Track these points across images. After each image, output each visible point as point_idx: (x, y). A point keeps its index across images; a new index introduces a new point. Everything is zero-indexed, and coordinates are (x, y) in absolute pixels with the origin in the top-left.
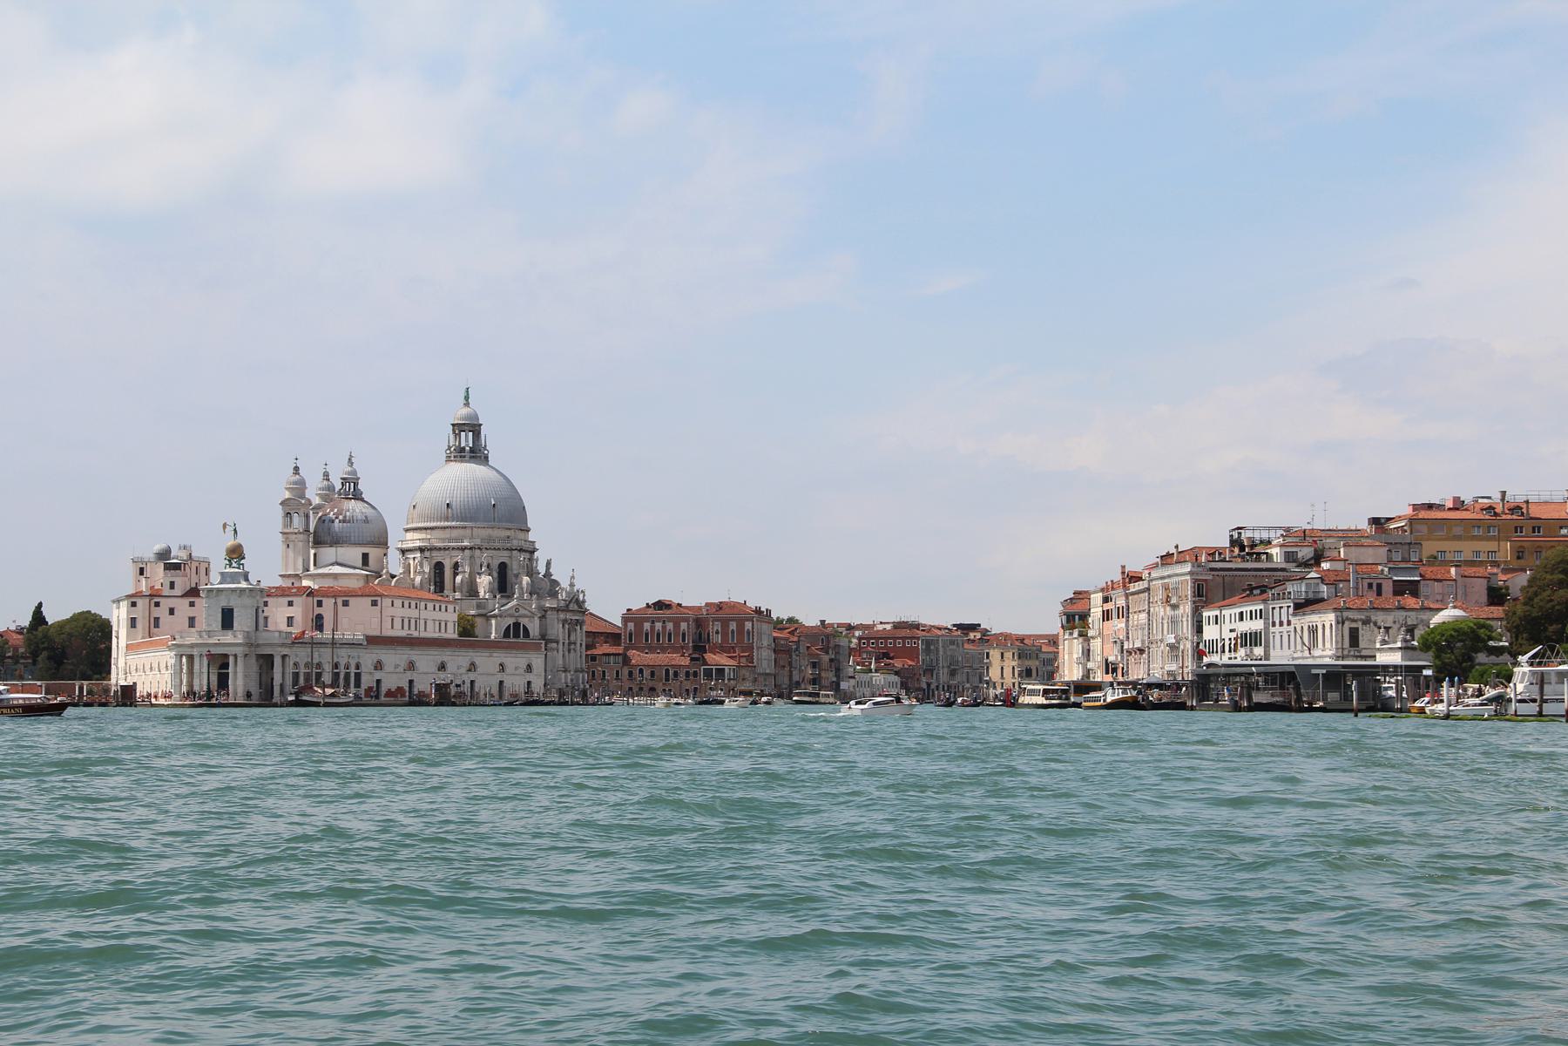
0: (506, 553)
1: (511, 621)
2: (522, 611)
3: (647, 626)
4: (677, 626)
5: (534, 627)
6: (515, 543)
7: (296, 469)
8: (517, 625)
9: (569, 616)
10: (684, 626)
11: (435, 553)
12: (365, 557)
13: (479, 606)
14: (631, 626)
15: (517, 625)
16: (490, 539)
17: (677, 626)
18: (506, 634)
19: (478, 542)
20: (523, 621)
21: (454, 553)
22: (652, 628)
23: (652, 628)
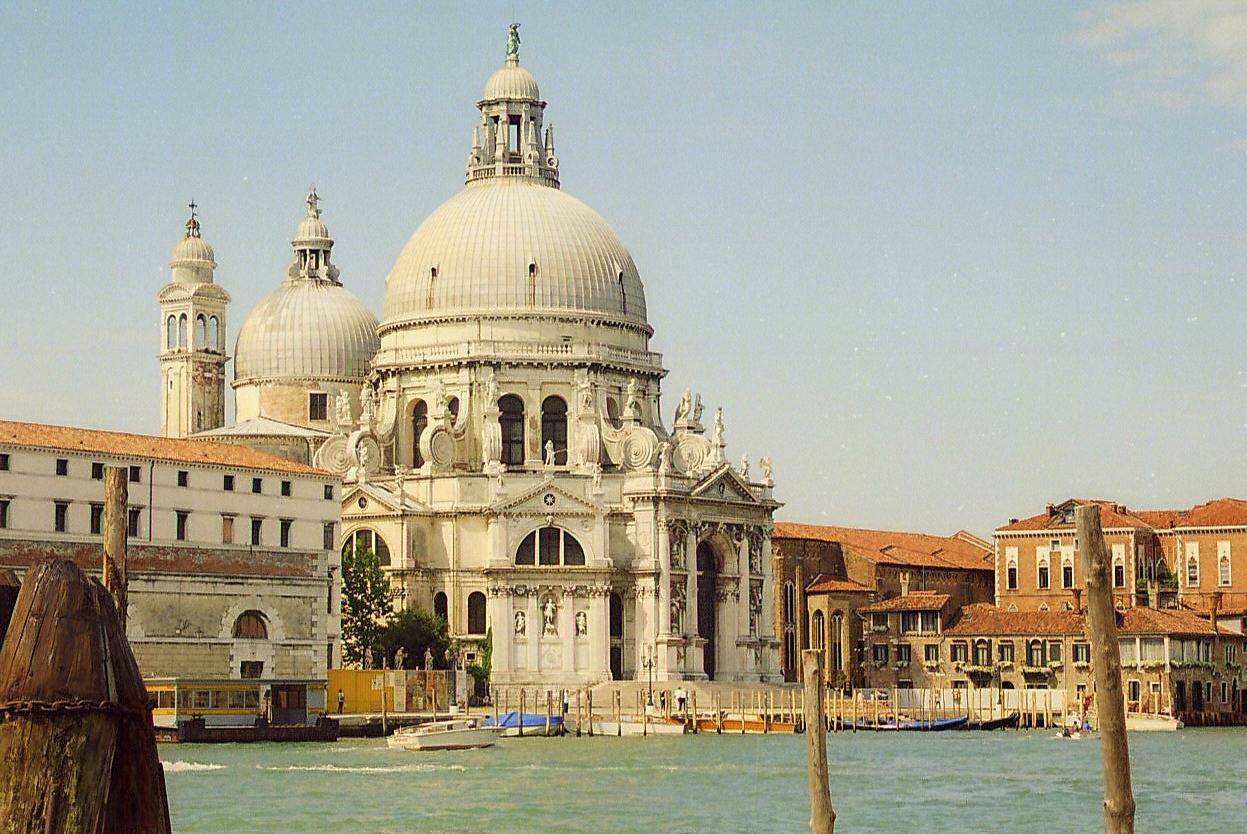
0: (560, 375)
1: (535, 525)
3: (1043, 553)
6: (579, 353)
7: (196, 225)
8: (550, 535)
9: (694, 515)
14: (1012, 554)
15: (550, 535)
18: (524, 552)
21: (449, 377)
22: (1055, 557)
23: (1055, 557)
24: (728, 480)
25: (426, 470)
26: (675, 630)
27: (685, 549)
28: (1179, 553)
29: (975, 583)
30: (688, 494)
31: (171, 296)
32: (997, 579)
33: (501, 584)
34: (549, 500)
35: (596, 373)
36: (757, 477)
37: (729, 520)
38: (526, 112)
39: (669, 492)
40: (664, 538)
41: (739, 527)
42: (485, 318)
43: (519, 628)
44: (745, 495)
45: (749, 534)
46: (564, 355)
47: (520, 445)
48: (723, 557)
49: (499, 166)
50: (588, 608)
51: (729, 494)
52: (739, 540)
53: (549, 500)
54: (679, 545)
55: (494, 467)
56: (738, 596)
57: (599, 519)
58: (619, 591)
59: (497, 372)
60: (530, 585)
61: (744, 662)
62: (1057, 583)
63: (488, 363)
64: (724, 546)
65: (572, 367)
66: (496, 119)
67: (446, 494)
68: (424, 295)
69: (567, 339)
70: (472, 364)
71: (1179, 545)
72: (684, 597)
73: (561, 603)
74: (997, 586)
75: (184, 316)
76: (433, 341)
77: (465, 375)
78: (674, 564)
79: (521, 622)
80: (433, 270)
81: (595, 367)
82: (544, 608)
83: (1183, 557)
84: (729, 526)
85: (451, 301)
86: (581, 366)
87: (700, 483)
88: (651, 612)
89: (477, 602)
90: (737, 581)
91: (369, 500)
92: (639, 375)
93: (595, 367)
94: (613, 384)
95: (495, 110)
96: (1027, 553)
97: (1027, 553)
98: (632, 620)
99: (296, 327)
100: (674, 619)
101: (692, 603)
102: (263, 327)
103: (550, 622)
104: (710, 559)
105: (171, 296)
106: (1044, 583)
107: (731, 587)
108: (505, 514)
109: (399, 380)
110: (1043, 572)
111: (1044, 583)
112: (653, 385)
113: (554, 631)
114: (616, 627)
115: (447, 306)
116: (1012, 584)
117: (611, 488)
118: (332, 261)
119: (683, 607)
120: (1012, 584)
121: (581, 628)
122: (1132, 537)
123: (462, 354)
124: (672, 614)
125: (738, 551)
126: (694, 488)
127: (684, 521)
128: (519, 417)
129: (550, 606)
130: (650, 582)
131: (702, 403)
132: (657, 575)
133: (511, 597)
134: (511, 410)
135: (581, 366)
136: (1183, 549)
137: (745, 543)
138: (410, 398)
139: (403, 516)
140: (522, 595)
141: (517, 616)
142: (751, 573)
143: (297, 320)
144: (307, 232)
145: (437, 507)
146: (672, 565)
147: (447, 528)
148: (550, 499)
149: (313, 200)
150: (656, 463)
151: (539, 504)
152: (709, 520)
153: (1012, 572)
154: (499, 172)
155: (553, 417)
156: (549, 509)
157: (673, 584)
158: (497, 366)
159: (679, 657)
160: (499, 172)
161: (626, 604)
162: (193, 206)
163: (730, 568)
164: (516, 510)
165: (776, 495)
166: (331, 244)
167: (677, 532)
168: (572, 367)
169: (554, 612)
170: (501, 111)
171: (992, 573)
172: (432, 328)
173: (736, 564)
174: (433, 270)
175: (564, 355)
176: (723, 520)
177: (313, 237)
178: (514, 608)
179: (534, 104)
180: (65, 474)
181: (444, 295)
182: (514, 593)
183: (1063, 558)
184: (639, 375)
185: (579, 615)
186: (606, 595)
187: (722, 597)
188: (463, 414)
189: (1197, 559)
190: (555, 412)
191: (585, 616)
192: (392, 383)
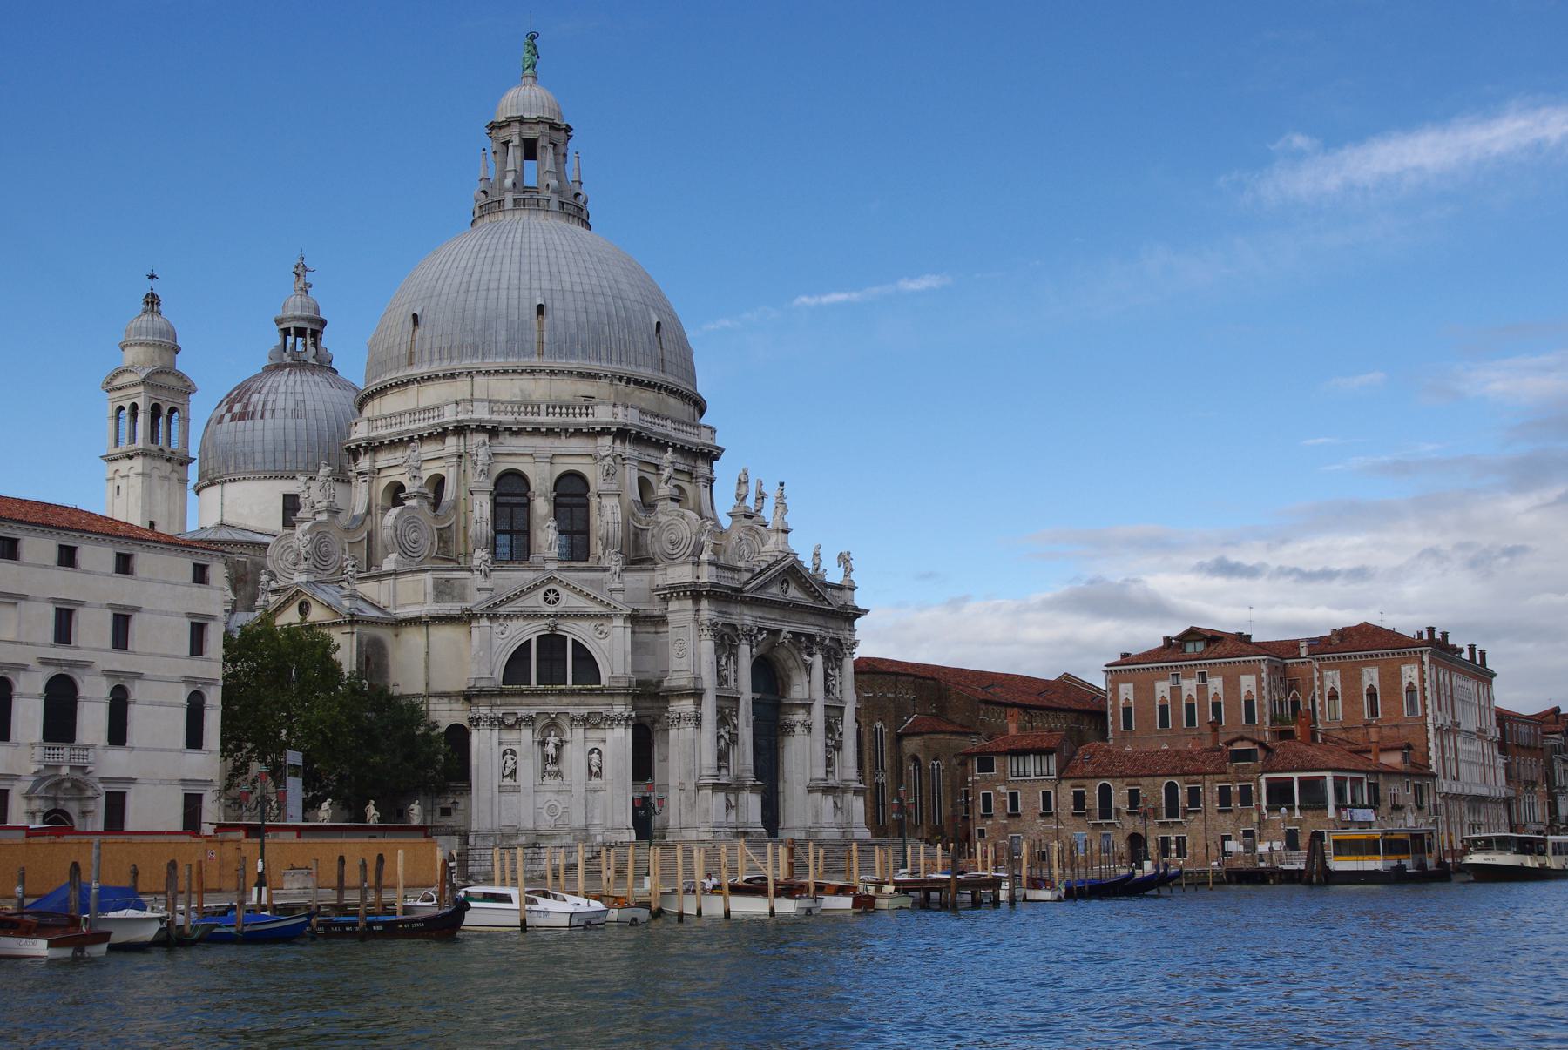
1: (530, 631)
2: (569, 601)
3: (1163, 688)
4: (1232, 684)
5: (613, 650)
6: (603, 415)
8: (552, 644)
9: (746, 618)
10: (1248, 683)
11: (384, 459)
12: (291, 504)
13: (442, 591)
14: (1126, 691)
15: (552, 644)
16: (530, 406)
17: (1232, 684)
19: (482, 413)
20: (576, 631)
21: (429, 450)
22: (1176, 691)
23: (1176, 691)
24: (792, 572)
25: (388, 564)
26: (724, 771)
27: (736, 663)
28: (1317, 683)
29: (1086, 726)
30: (740, 590)
31: (118, 382)
32: (1110, 719)
33: (484, 711)
34: (551, 596)
35: (623, 442)
36: (834, 575)
37: (797, 628)
38: (539, 140)
39: (713, 585)
40: (708, 645)
41: (810, 637)
42: (479, 372)
43: (507, 772)
44: (817, 596)
45: (823, 648)
46: (584, 419)
47: (524, 540)
48: (789, 677)
49: (509, 197)
50: (604, 741)
51: (794, 593)
52: (810, 655)
53: (551, 596)
54: (728, 658)
55: (480, 556)
56: (809, 727)
57: (619, 622)
58: (647, 721)
59: (494, 442)
60: (522, 712)
61: (817, 814)
62: (1178, 719)
63: (481, 428)
64: (791, 663)
65: (593, 434)
66: (506, 143)
67: (412, 594)
68: (404, 350)
69: (589, 398)
70: (461, 430)
71: (1317, 675)
72: (736, 727)
73: (567, 737)
74: (1110, 727)
75: (134, 407)
76: (412, 405)
77: (452, 444)
78: (722, 679)
79: (510, 763)
80: (415, 316)
81: (622, 434)
82: (543, 743)
83: (1321, 687)
84: (796, 635)
85: (436, 356)
86: (605, 432)
87: (755, 576)
88: (689, 748)
89: (459, 736)
90: (807, 706)
91: (312, 603)
92: (681, 450)
93: (622, 434)
94: (648, 459)
95: (503, 134)
96: (1143, 690)
97: (1143, 690)
98: (666, 759)
99: (268, 414)
100: (722, 756)
101: (746, 734)
102: (228, 416)
103: (552, 762)
104: (769, 675)
105: (118, 382)
106: (1164, 723)
107: (800, 716)
108: (488, 617)
109: (373, 461)
110: (1163, 709)
111: (1164, 723)
112: (702, 468)
113: (558, 774)
114: (643, 766)
115: (431, 361)
116: (1128, 724)
117: (639, 581)
118: (323, 344)
119: (734, 740)
120: (1128, 724)
121: (595, 769)
122: (1263, 666)
123: (450, 416)
124: (719, 750)
125: (809, 668)
126: (746, 583)
127: (734, 627)
128: (524, 500)
129: (552, 740)
130: (686, 706)
131: (764, 490)
132: (697, 695)
133: (496, 731)
134: (510, 490)
135: (605, 432)
136: (1321, 679)
137: (818, 661)
138: (384, 482)
139: (352, 622)
140: (511, 727)
141: (505, 753)
142: (827, 698)
143: (269, 407)
144: (295, 307)
145: (402, 613)
146: (720, 684)
147: (414, 638)
148: (552, 597)
149: (300, 271)
150: (698, 550)
151: (536, 601)
152: (768, 626)
153: (1127, 711)
154: (509, 204)
155: (565, 500)
156: (551, 609)
157: (720, 710)
158: (493, 432)
159: (728, 806)
160: (509, 204)
161: (657, 739)
162: (152, 277)
163: (798, 690)
164: (502, 610)
165: (859, 600)
166: (323, 323)
167: (726, 641)
168: (593, 434)
169: (558, 747)
170: (514, 135)
171: (1105, 715)
172: (413, 388)
173: (807, 686)
174: (415, 316)
175: (584, 419)
176: (786, 628)
177: (298, 313)
178: (500, 743)
179: (553, 126)
180: (201, 654)
181: (427, 346)
182: (499, 723)
183: (1185, 695)
184: (681, 450)
185: (592, 752)
186: (627, 725)
187: (788, 730)
188: (449, 494)
189: (1339, 690)
190: (572, 494)
191: (600, 753)
192: (364, 463)
